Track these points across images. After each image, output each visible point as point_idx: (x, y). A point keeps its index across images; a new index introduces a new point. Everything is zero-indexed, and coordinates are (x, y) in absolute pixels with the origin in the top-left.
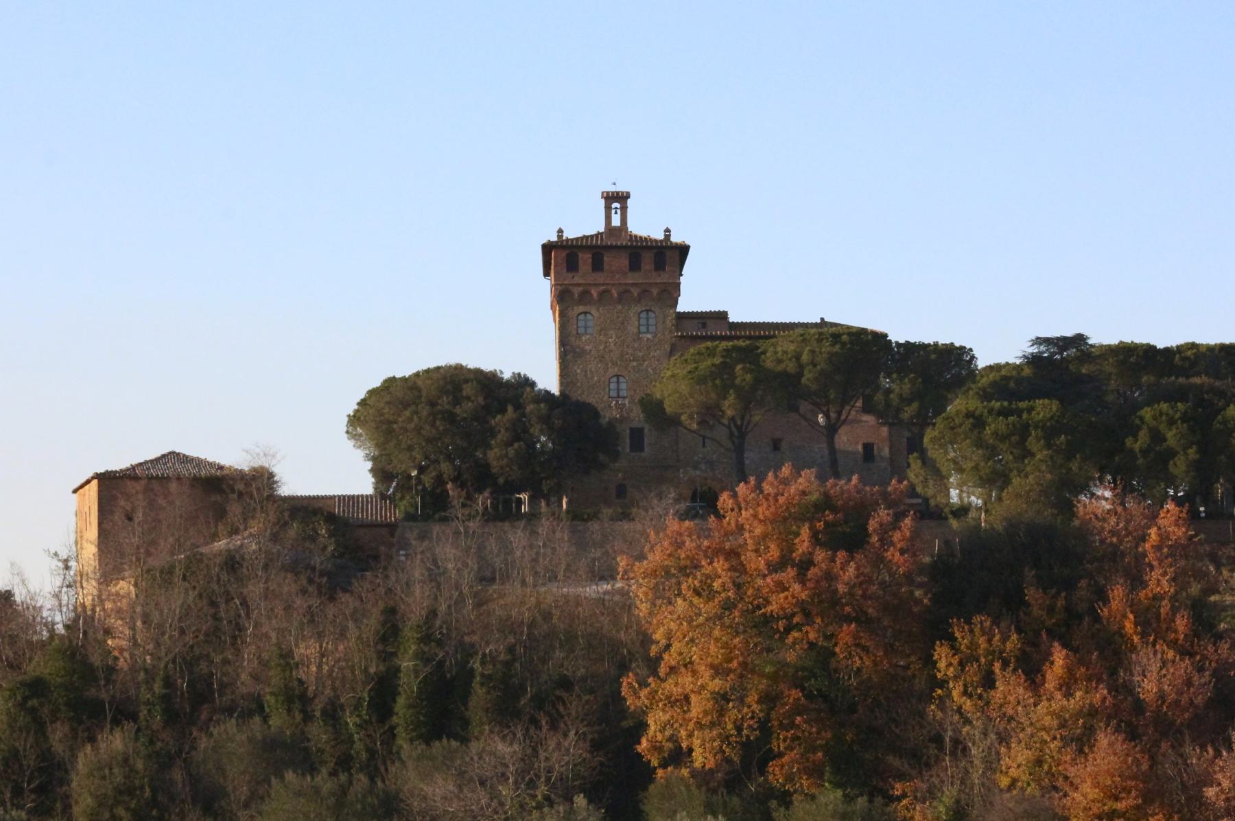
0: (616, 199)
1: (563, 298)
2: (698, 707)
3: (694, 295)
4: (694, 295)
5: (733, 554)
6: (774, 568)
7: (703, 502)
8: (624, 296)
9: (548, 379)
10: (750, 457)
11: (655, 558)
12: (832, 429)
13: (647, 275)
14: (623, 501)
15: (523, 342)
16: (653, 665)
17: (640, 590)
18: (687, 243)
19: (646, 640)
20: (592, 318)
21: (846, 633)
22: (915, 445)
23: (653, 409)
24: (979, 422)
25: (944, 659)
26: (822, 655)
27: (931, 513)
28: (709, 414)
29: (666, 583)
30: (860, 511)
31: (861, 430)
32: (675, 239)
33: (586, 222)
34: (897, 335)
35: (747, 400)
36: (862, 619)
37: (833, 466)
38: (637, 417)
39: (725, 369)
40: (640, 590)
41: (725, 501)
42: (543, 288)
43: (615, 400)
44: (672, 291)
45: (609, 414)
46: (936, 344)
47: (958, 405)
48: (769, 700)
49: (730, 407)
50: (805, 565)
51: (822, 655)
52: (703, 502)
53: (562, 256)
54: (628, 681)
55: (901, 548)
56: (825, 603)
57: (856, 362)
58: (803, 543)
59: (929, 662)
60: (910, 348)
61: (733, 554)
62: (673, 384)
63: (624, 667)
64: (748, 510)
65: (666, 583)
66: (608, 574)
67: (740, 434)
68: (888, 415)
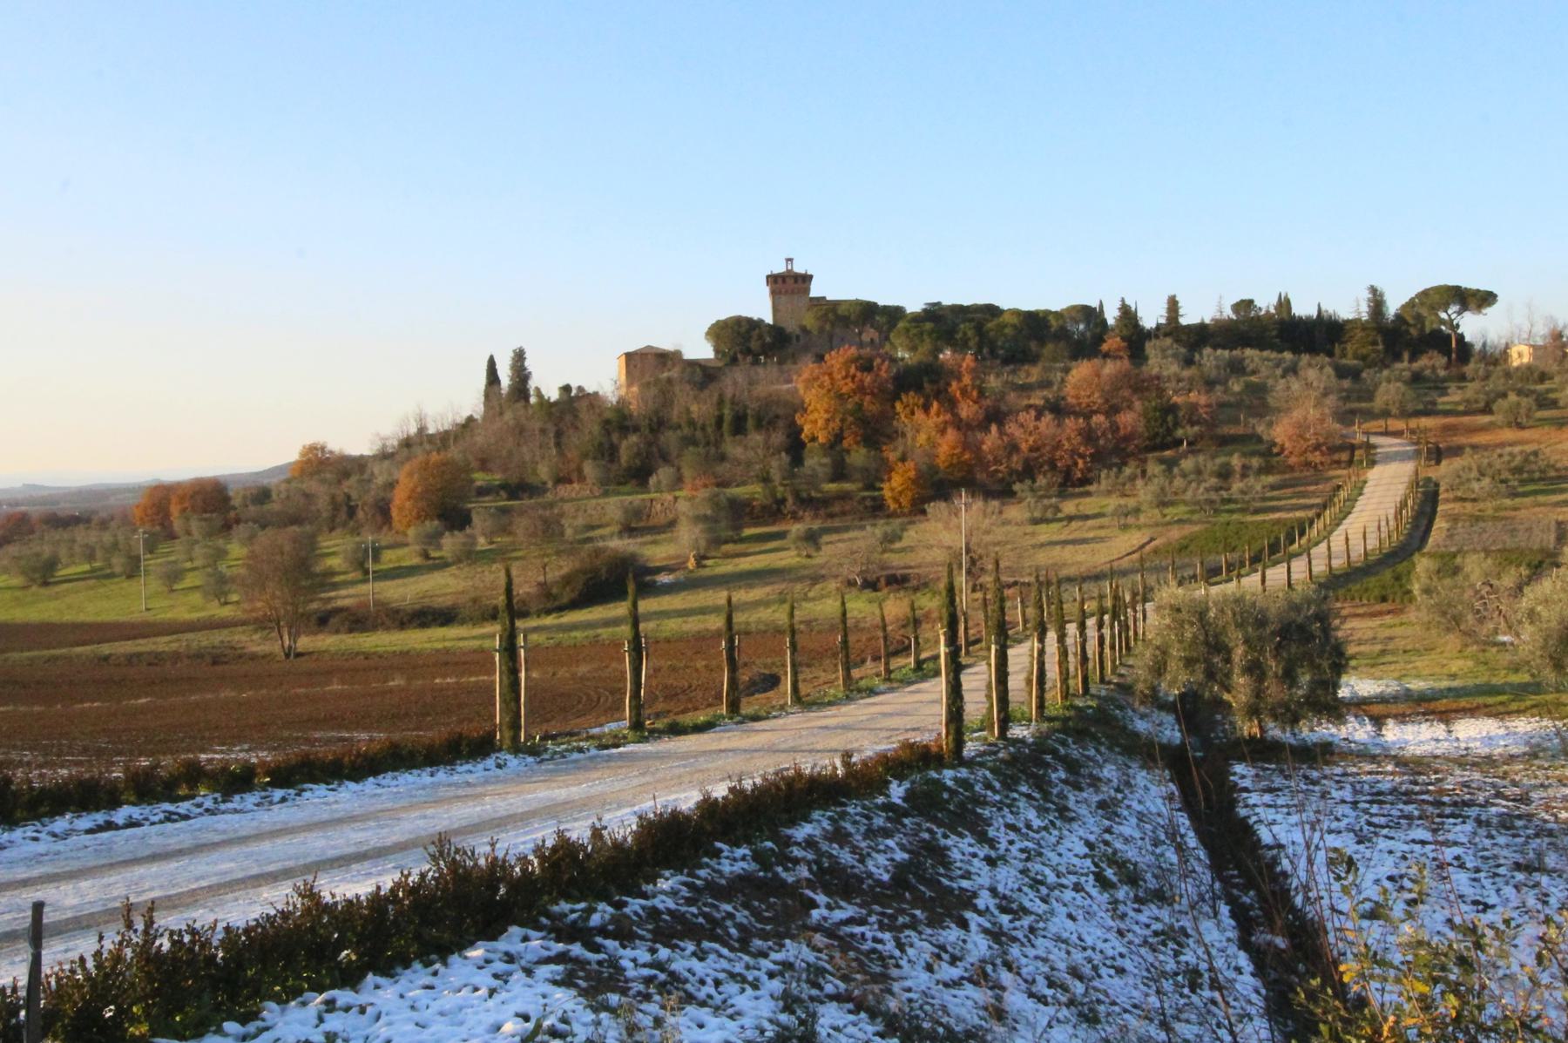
0: (789, 260)
1: (773, 293)
2: (820, 423)
3: (816, 291)
4: (816, 291)
5: (830, 374)
6: (846, 377)
7: (820, 358)
8: (793, 292)
9: (769, 320)
10: (835, 342)
11: (806, 375)
12: (860, 334)
13: (800, 285)
14: (794, 359)
15: (760, 308)
16: (805, 410)
17: (801, 387)
19: (803, 402)
20: (784, 299)
21: (868, 398)
22: (887, 338)
23: (804, 329)
24: (908, 330)
25: (898, 406)
26: (860, 406)
27: (894, 360)
28: (821, 330)
29: (809, 383)
30: (871, 360)
31: (870, 334)
33: (780, 268)
34: (881, 303)
35: (833, 325)
36: (872, 394)
37: (861, 345)
38: (798, 331)
39: (826, 315)
40: (801, 387)
41: (827, 357)
42: (767, 290)
43: (791, 326)
44: (807, 290)
45: (789, 330)
47: (901, 325)
48: (843, 420)
49: (828, 327)
50: (854, 377)
51: (860, 406)
52: (820, 358)
53: (773, 280)
54: (797, 416)
55: (885, 372)
56: (861, 389)
57: (868, 311)
58: (853, 370)
59: (893, 407)
60: (885, 307)
61: (830, 374)
62: (809, 321)
63: (795, 411)
64: (837, 359)
65: (809, 383)
66: (789, 381)
67: (831, 337)
68: (879, 329)
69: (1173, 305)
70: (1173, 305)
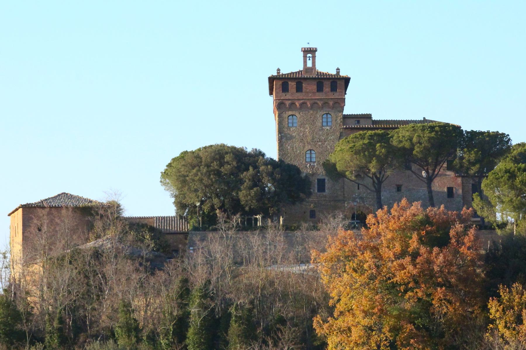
0: (309, 52)
1: (280, 107)
2: (356, 333)
3: (354, 104)
4: (354, 104)
5: (375, 249)
6: (400, 256)
7: (359, 220)
8: (314, 105)
9: (272, 152)
10: (384, 195)
11: (332, 251)
12: (430, 179)
13: (327, 94)
14: (314, 218)
15: (258, 132)
16: (331, 311)
17: (323, 269)
18: (349, 76)
19: (327, 297)
20: (297, 118)
21: (440, 292)
22: (477, 188)
23: (330, 168)
24: (512, 176)
25: (493, 306)
26: (425, 306)
27: (485, 226)
28: (362, 172)
29: (337, 265)
30: (446, 225)
31: (446, 180)
32: (343, 74)
33: (293, 65)
34: (466, 127)
35: (382, 163)
36: (448, 285)
37: (431, 200)
38: (321, 172)
39: (371, 146)
40: (323, 269)
41: (370, 219)
42: (269, 102)
43: (309, 164)
44: (340, 103)
45: (306, 171)
46: (488, 132)
47: (501, 166)
48: (395, 330)
49: (373, 167)
50: (415, 255)
51: (425, 306)
52: (359, 220)
53: (279, 83)
54: (317, 320)
55: (469, 246)
56: (427, 276)
57: (445, 141)
58: (414, 243)
59: (485, 309)
60: (473, 134)
61: (375, 249)
62: (342, 155)
63: (314, 312)
64: (387, 224)
65: (337, 265)
66: (306, 260)
67: (378, 183)
68: (461, 171)
69: (279, 70)
70: (279, 70)
